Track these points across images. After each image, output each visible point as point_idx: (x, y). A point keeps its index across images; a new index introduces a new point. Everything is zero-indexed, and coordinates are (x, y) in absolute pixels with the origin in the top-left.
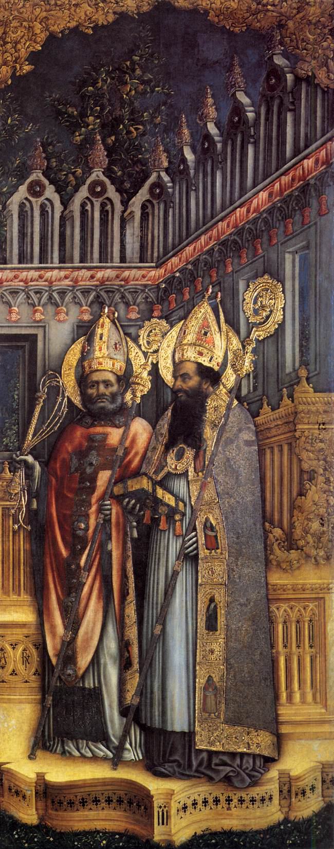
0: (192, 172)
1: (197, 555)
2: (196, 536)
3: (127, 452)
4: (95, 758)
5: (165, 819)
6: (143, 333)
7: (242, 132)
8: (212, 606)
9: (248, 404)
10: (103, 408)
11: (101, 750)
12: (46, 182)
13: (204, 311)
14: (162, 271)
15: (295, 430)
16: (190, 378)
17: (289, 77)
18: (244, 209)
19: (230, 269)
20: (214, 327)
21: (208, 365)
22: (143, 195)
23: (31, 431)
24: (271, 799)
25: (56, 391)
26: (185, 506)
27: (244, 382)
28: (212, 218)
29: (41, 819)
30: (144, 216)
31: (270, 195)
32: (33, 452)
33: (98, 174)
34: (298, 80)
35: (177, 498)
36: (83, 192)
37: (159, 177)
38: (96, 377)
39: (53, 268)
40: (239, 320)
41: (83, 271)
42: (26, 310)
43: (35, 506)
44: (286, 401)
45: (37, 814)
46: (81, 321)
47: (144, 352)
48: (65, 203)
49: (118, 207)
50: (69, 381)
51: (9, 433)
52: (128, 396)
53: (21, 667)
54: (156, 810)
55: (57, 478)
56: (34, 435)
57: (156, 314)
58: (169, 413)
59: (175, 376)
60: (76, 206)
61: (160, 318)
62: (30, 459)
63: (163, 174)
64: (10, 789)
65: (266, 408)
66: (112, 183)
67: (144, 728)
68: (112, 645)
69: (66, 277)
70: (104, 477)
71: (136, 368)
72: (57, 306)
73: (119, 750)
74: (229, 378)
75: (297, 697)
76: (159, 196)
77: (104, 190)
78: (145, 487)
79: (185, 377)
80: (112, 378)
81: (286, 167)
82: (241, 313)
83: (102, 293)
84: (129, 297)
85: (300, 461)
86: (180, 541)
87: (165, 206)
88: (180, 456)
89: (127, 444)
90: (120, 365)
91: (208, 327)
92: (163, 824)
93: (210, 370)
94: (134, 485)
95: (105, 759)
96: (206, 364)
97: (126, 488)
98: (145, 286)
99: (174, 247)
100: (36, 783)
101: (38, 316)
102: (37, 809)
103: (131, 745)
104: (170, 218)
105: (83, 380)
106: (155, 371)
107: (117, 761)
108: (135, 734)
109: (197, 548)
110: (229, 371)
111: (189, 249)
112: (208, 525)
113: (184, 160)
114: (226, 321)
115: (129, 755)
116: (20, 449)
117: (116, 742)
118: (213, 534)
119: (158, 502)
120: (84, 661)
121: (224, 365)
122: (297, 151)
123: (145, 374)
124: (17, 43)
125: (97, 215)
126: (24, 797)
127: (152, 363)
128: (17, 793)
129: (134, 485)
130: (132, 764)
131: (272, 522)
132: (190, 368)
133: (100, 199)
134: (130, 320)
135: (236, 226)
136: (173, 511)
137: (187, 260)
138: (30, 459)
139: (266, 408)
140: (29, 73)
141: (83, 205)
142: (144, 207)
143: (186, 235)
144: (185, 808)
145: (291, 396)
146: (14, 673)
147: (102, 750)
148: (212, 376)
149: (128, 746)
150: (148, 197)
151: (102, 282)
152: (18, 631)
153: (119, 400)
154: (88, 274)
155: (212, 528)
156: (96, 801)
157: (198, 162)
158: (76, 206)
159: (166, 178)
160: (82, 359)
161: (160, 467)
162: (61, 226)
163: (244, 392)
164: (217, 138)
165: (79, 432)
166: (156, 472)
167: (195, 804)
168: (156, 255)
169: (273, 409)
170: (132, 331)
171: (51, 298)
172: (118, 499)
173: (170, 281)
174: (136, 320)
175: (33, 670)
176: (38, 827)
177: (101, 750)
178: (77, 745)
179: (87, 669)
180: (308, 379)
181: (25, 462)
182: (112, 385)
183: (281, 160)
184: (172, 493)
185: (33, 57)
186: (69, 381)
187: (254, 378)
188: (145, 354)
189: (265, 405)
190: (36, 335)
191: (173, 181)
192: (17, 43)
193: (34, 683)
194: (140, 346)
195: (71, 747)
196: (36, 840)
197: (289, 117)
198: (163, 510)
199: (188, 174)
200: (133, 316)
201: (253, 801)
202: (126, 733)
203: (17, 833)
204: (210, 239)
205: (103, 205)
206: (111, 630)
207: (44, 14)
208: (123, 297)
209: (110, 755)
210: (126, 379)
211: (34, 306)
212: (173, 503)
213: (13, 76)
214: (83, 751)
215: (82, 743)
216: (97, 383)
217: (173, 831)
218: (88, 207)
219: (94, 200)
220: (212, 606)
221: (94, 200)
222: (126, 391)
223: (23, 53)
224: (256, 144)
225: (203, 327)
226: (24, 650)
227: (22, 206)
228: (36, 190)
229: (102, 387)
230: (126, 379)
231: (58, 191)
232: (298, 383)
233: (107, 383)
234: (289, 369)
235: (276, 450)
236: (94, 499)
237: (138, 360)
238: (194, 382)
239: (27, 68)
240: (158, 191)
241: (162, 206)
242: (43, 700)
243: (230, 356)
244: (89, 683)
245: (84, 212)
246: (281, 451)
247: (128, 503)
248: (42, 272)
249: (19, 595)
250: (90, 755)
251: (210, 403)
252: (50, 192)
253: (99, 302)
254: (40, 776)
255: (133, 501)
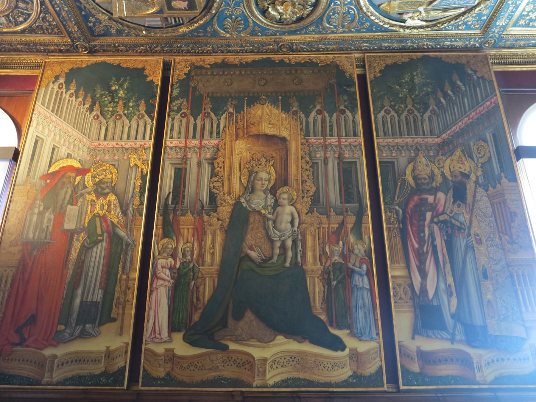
0: (445, 106)
1: (473, 246)
2: (471, 238)
3: (437, 205)
4: (442, 338)
5: (480, 369)
6: (436, 161)
7: (462, 94)
8: (484, 268)
9: (483, 187)
10: (424, 188)
11: (444, 334)
12: (391, 110)
13: (458, 152)
14: (439, 139)
15: (504, 196)
16: (458, 177)
17: (475, 77)
18: (467, 118)
19: (466, 138)
20: (464, 159)
21: (465, 172)
22: (428, 114)
23: (396, 197)
24: (528, 358)
25: (404, 181)
26: (465, 226)
27: (480, 178)
28: (456, 121)
29: (421, 369)
30: (430, 120)
31: (476, 114)
32: (398, 205)
33: (410, 107)
34: (478, 78)
35: (461, 223)
36: (405, 113)
37: (433, 108)
38: (420, 176)
39: (397, 138)
40: (473, 155)
41: (409, 139)
42: (389, 152)
43: (401, 226)
44: (498, 185)
45: (419, 367)
46: (411, 156)
47: (437, 167)
48: (399, 116)
49: (420, 118)
50: (409, 178)
51: (387, 198)
52: (434, 184)
53: (403, 296)
54: (475, 365)
55: (409, 215)
56: (398, 198)
57: (440, 154)
58: (451, 190)
59: (451, 176)
60: (403, 117)
61: (442, 155)
62: (397, 207)
63: (434, 107)
64: (405, 355)
65: (491, 188)
66: (416, 110)
67: (464, 325)
68: (442, 286)
69: (403, 141)
70: (429, 215)
71: (436, 174)
72: (400, 151)
73: (453, 335)
74: (473, 177)
75: (530, 309)
76: (434, 114)
77: (413, 112)
78: (447, 218)
79: (456, 176)
80: (426, 177)
81: (480, 105)
82: (474, 154)
83: (418, 146)
84: (429, 148)
85: (509, 208)
86: (465, 240)
87: (437, 117)
88: (459, 206)
89: (436, 202)
90: (429, 171)
91: (462, 158)
92: (479, 371)
93: (465, 174)
94: (442, 218)
95: (447, 339)
96: (463, 171)
97: (438, 219)
98: (435, 144)
99: (443, 131)
100: (417, 351)
101: (394, 155)
102: (418, 365)
103: (458, 332)
104: (440, 121)
105: (415, 178)
106: (443, 174)
107: (452, 340)
108: (459, 327)
109: (473, 244)
110: (473, 174)
111: (449, 132)
112: (476, 234)
113: (442, 102)
114: (468, 156)
115: (458, 337)
116: (392, 203)
117: (451, 331)
118: (478, 238)
119: (453, 225)
120: (431, 294)
121: (470, 172)
122: (483, 100)
123: (439, 176)
124: (375, 67)
125: (412, 120)
126: (412, 358)
127: (442, 171)
128: (408, 356)
129: (442, 218)
130: (460, 342)
131: (503, 233)
132: (457, 173)
133: (412, 115)
134: (430, 156)
135: (466, 123)
136: (460, 228)
137: (449, 135)
138: (397, 207)
139: (491, 188)
140: (380, 76)
141: (406, 117)
142: (429, 117)
143: (447, 127)
144: (488, 363)
145: (500, 183)
146: (400, 298)
147: (444, 334)
148: (467, 176)
149: (457, 332)
150: (430, 114)
151: (417, 143)
152: (401, 280)
153: (430, 185)
154: (411, 140)
155: (478, 235)
156: (446, 360)
157: (446, 103)
158: (403, 117)
159: (436, 108)
160: (413, 170)
161: (452, 211)
162: (398, 124)
163: (480, 182)
164: (452, 96)
165: (416, 198)
166: (451, 213)
167: (493, 361)
168: (436, 133)
169: (494, 188)
170: (432, 160)
171: (398, 148)
172: (437, 223)
173: (444, 142)
174: (433, 156)
175: (409, 297)
176: (420, 373)
177: (444, 334)
178: (433, 332)
179: (433, 297)
180: (505, 177)
181: (395, 209)
182: (427, 180)
183: (478, 103)
184: (458, 221)
185: (381, 71)
186: (409, 178)
187: (484, 177)
188: (439, 168)
189: (490, 187)
190: (393, 162)
191: (438, 109)
192: (375, 67)
193: (411, 303)
194: (436, 165)
195: (430, 333)
196: (420, 380)
197: (478, 89)
198: (456, 228)
199: (444, 107)
200: (431, 154)
201: (520, 359)
202: (455, 326)
203: (410, 377)
204: (456, 128)
205: (413, 117)
206: (441, 279)
207: (383, 59)
208: (426, 148)
209: (449, 337)
210: (432, 177)
211: (392, 151)
212: (459, 225)
213: (375, 77)
214: (437, 336)
215: (436, 331)
216: (421, 179)
217: (485, 375)
218: (408, 118)
219: (410, 115)
220: (484, 268)
221: (410, 115)
222: (433, 182)
223: (377, 70)
224: (467, 97)
225: (459, 158)
226: (404, 288)
227: (383, 118)
228: (387, 112)
229: (423, 180)
230: (432, 177)
231: (396, 112)
232: (501, 179)
233: (425, 179)
234: (497, 173)
235: (498, 204)
236: (427, 223)
237: (436, 171)
238: (460, 178)
239: (379, 75)
240: (433, 112)
241: (436, 117)
242: (415, 311)
243: (473, 169)
244: (435, 303)
245: (406, 119)
246: (500, 205)
247: (441, 225)
248: (394, 139)
249: (399, 263)
250: (440, 337)
251: (468, 187)
252: (393, 113)
253: (417, 150)
254: (418, 348)
255: (443, 225)
